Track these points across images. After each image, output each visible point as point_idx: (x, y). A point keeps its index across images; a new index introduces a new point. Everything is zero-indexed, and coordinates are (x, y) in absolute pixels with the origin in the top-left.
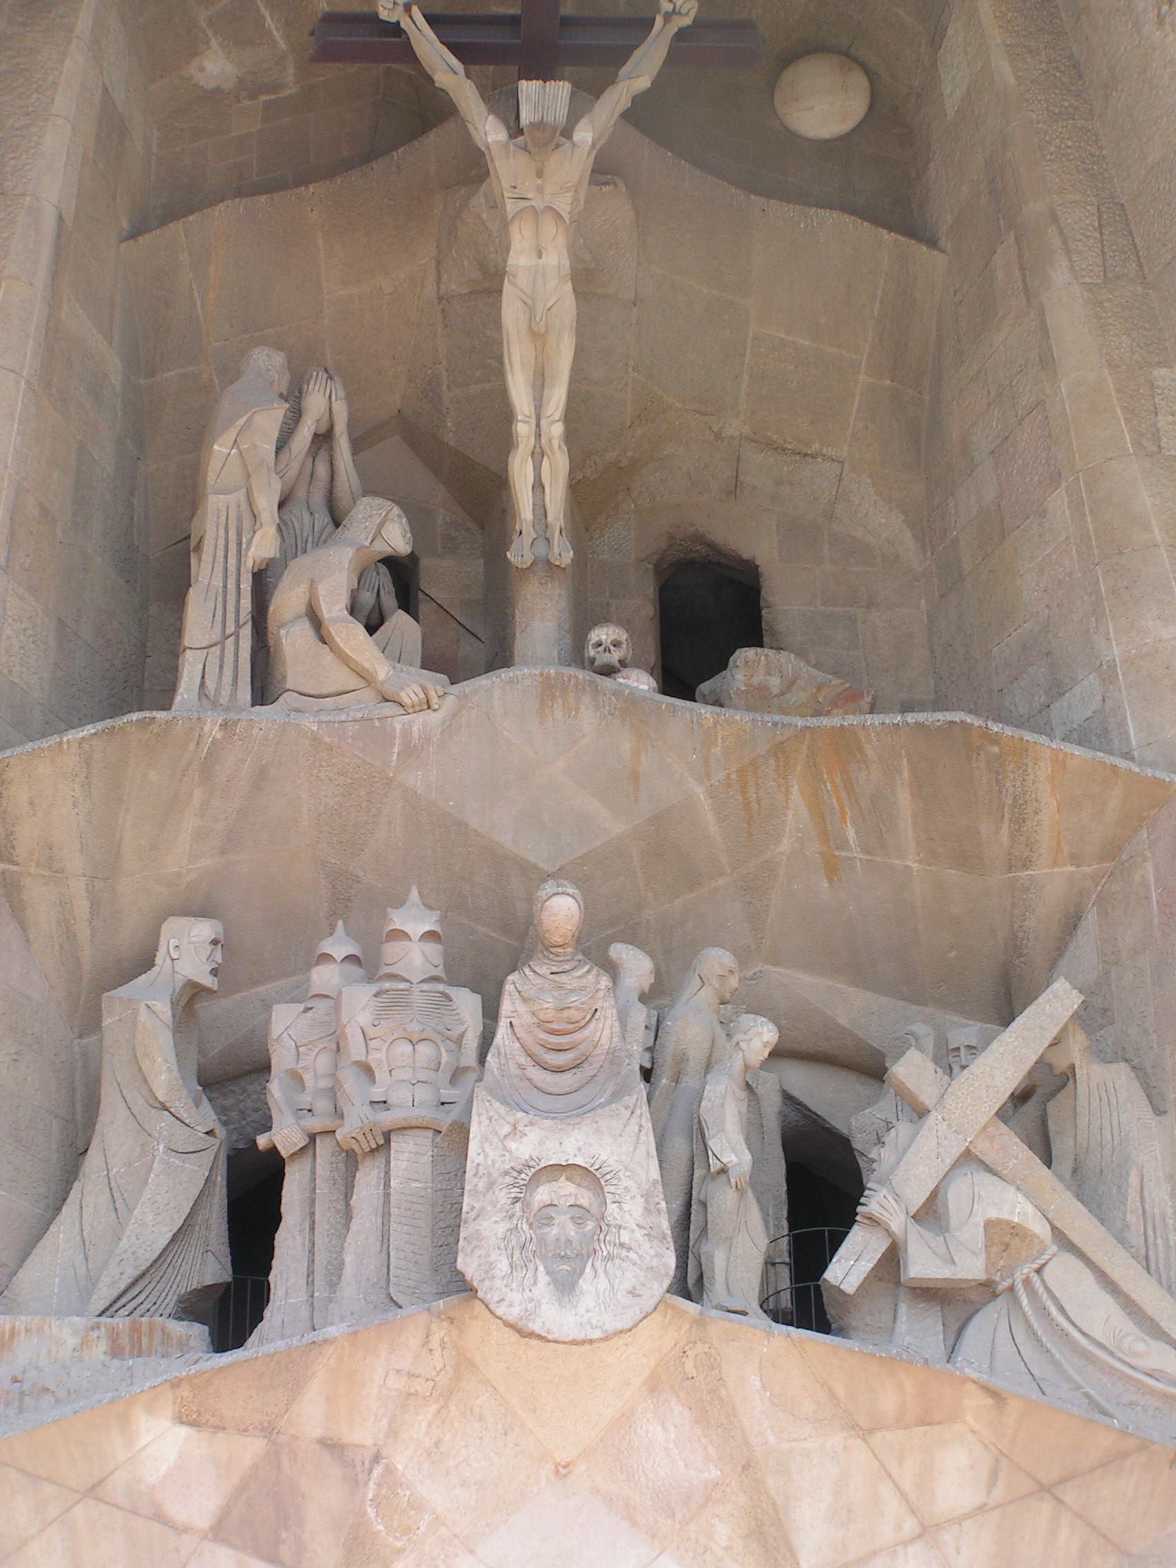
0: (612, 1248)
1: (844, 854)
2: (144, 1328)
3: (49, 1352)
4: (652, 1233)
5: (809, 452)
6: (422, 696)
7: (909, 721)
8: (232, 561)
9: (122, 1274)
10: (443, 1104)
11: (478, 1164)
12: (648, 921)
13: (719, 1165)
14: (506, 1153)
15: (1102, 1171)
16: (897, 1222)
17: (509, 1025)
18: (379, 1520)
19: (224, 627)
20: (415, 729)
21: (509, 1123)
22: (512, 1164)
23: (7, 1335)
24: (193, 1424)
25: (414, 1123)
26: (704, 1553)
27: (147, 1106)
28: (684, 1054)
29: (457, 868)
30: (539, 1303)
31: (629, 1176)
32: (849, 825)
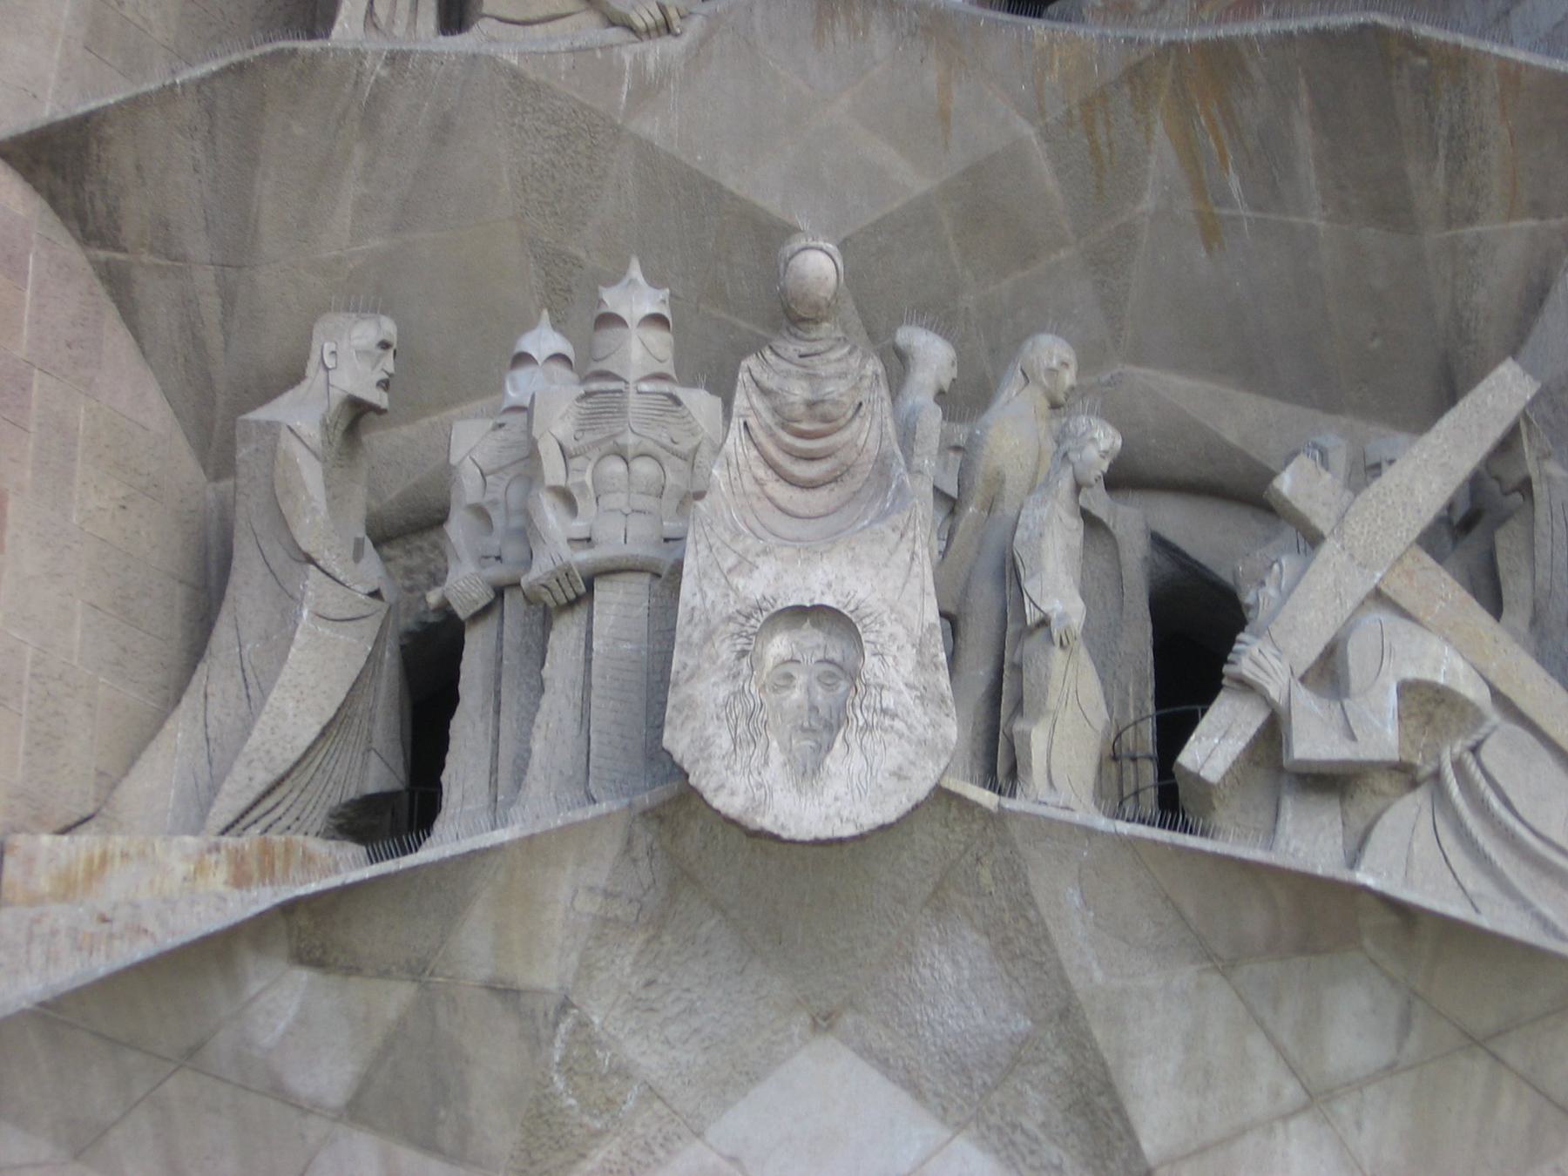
0: (871, 715)
1: (1226, 212)
2: (279, 850)
3: (152, 883)
6: (659, 16)
9: (251, 779)
10: (666, 540)
13: (1038, 615)
14: (732, 594)
18: (570, 1092)
22: (738, 607)
23: (96, 861)
24: (319, 964)
25: (623, 564)
28: (998, 474)
31: (896, 620)
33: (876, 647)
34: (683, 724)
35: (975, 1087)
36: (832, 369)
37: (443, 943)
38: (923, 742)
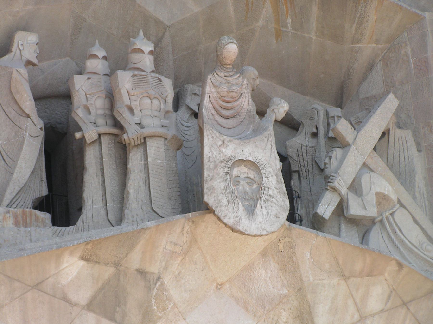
1: (285, 29)
2: (28, 214)
4: (280, 191)
9: (14, 189)
10: (162, 126)
11: (209, 157)
12: (201, 49)
14: (221, 153)
15: (400, 174)
16: (344, 191)
17: (208, 97)
18: (156, 305)
21: (221, 140)
22: (224, 158)
24: (87, 260)
25: (157, 134)
27: (17, 115)
29: (128, 20)
30: (241, 219)
31: (270, 167)
32: (289, 18)
33: (266, 175)
34: (211, 194)
35: (266, 309)
36: (234, 82)
37: (126, 256)
38: (281, 206)
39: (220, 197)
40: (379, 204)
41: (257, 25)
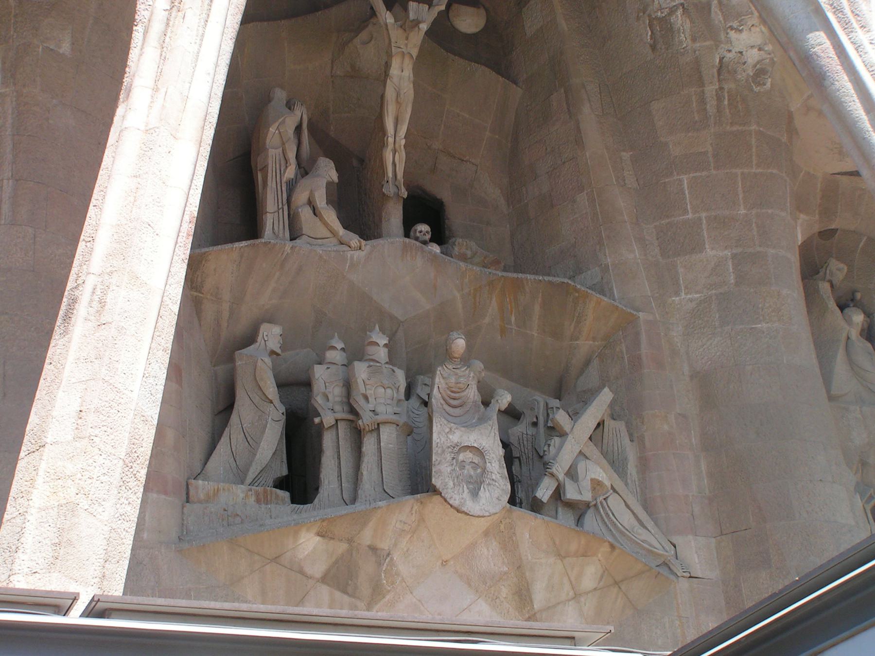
1: (509, 327)
2: (269, 492)
3: (233, 499)
5: (465, 159)
6: (358, 244)
7: (546, 279)
8: (278, 177)
10: (395, 414)
11: (438, 443)
14: (449, 440)
15: (613, 462)
16: (561, 477)
19: (278, 206)
20: (355, 257)
22: (451, 444)
24: (322, 536)
26: (496, 599)
30: (465, 501)
35: (487, 585)
36: (462, 374)
38: (503, 490)
39: (447, 480)
40: (594, 489)
41: (484, 322)
